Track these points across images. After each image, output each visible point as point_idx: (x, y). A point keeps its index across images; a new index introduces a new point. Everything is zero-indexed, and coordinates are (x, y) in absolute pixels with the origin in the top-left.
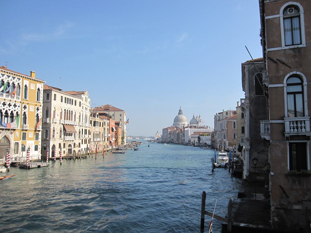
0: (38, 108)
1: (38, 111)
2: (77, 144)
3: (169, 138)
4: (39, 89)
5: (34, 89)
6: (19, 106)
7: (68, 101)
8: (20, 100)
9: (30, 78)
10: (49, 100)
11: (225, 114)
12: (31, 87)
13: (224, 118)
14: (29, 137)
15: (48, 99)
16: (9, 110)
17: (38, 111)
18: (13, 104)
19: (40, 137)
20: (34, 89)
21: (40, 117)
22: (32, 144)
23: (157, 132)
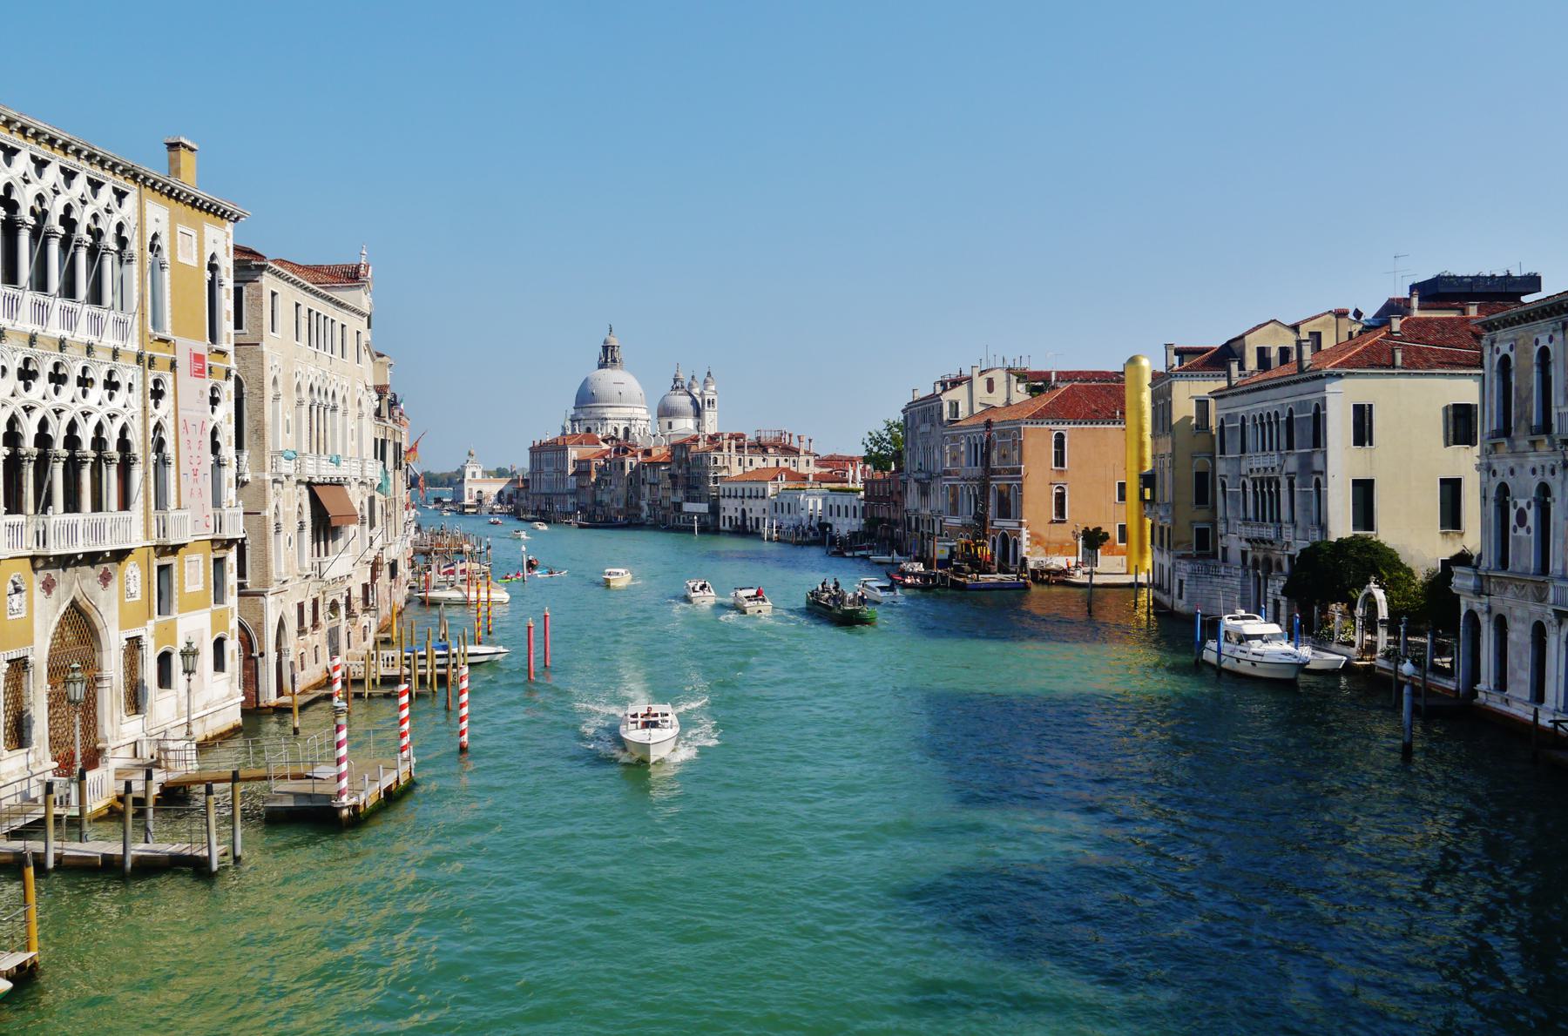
0: (213, 390)
1: (213, 410)
2: (357, 593)
3: (574, 493)
4: (213, 268)
5: (193, 262)
6: (130, 385)
7: (315, 331)
8: (133, 346)
9: (173, 182)
10: (245, 330)
11: (980, 384)
12: (179, 252)
13: (978, 409)
14: (189, 589)
15: (241, 328)
16: (86, 414)
17: (213, 410)
18: (98, 375)
19: (232, 578)
20: (193, 262)
21: (228, 451)
22: (202, 630)
23: (470, 454)
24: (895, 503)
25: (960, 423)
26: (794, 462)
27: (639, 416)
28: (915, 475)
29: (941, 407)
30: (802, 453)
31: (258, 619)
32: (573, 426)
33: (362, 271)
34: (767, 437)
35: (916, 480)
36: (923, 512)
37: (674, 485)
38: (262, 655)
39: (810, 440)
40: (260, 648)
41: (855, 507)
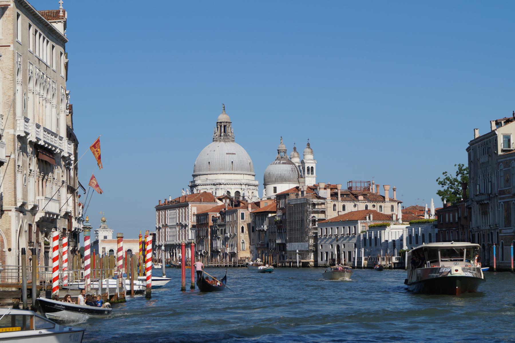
24: (463, 226)
25: (512, 152)
26: (381, 207)
27: (247, 182)
28: (477, 198)
29: (496, 140)
30: (386, 200)
31: (5, 227)
32: (192, 191)
33: (61, 14)
34: (357, 187)
35: (478, 202)
36: (484, 229)
37: (279, 228)
38: (10, 250)
39: (394, 190)
40: (8, 245)
41: (430, 235)
